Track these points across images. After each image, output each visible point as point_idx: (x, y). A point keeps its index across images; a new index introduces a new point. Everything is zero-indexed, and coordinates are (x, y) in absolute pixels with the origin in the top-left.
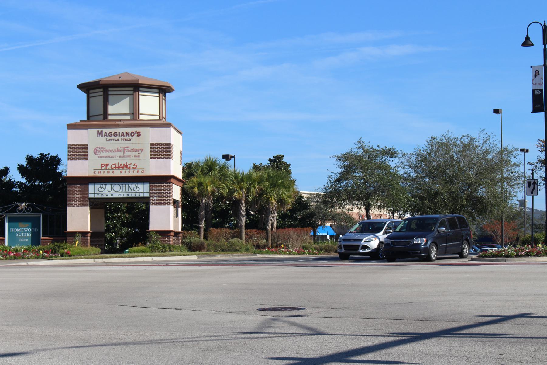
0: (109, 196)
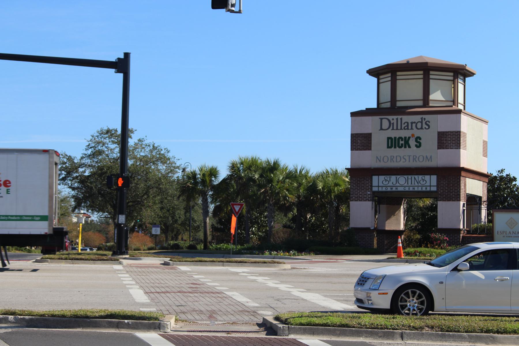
0: (394, 189)
